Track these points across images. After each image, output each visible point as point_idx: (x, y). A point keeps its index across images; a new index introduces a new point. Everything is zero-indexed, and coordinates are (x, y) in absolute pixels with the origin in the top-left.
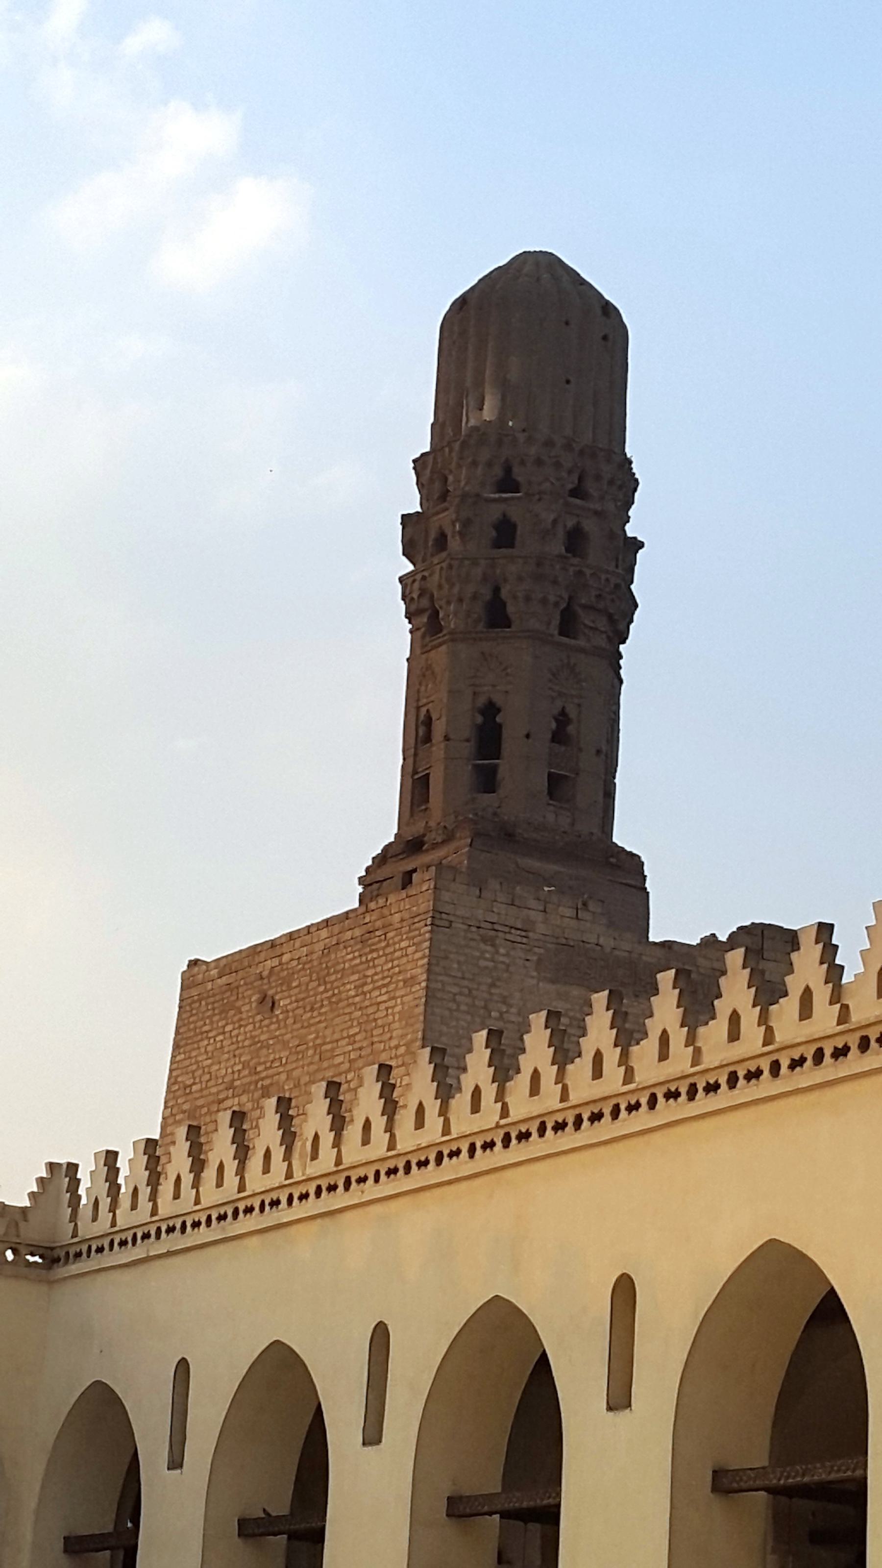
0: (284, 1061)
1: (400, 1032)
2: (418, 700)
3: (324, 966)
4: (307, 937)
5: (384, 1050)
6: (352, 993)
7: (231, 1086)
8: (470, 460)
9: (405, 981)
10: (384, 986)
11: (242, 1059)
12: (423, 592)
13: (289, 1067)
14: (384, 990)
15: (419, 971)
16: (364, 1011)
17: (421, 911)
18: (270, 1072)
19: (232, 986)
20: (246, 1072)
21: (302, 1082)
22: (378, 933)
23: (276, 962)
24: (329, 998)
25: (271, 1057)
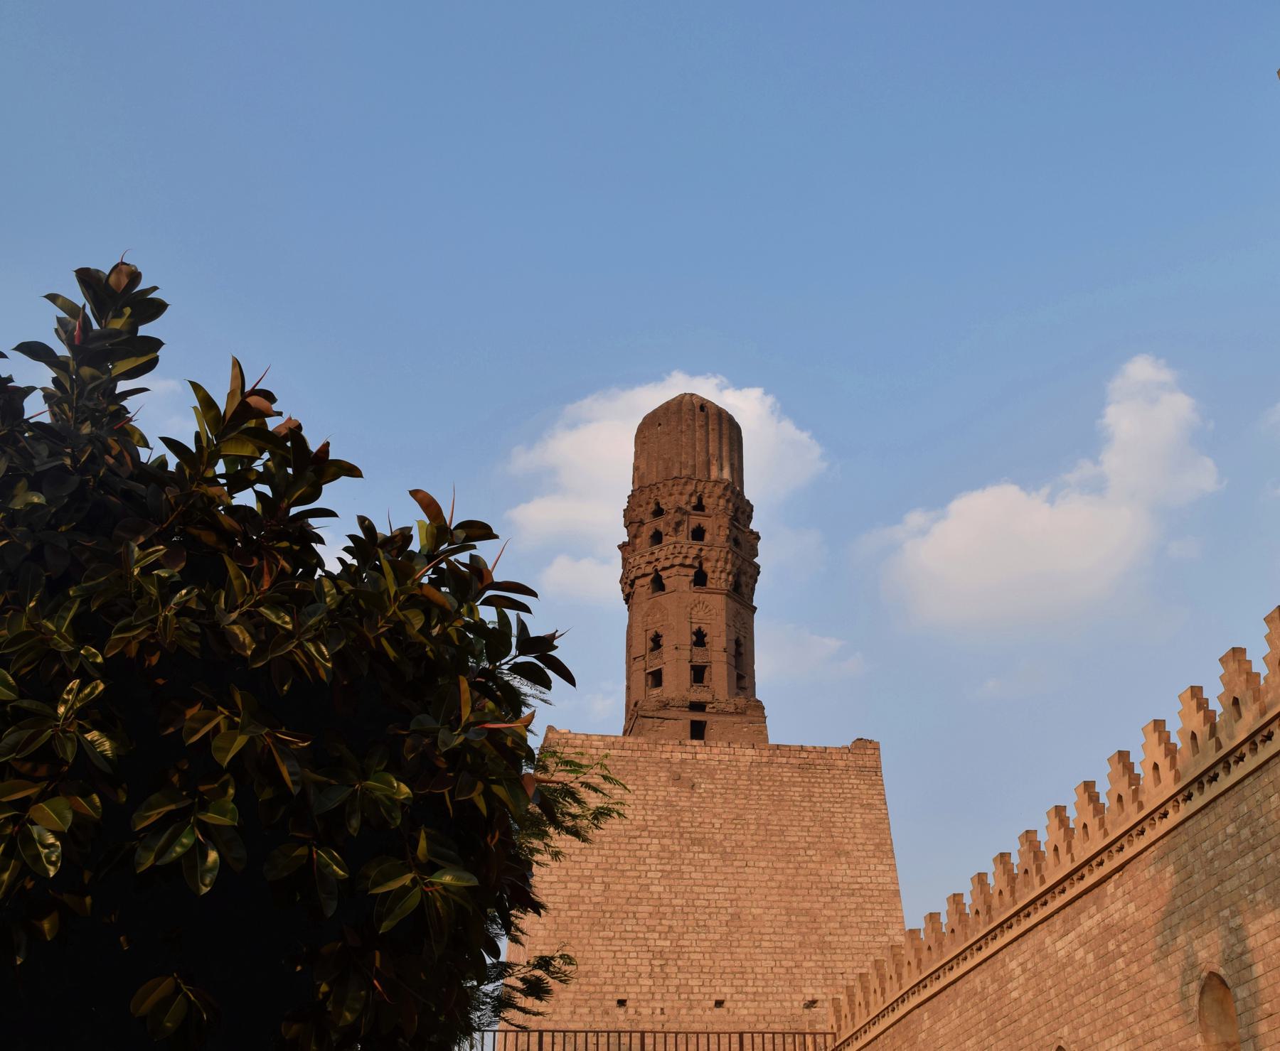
0: (717, 826)
1: (865, 836)
2: (691, 618)
3: (756, 773)
4: (727, 749)
5: (848, 843)
6: (799, 799)
7: (644, 828)
8: (726, 498)
9: (862, 805)
10: (837, 802)
11: (656, 813)
12: (697, 557)
13: (726, 831)
14: (836, 805)
15: (877, 802)
16: (816, 814)
17: (868, 765)
18: (698, 830)
19: (627, 759)
20: (666, 824)
21: (746, 844)
22: (818, 767)
23: (685, 756)
24: (768, 796)
25: (700, 820)
